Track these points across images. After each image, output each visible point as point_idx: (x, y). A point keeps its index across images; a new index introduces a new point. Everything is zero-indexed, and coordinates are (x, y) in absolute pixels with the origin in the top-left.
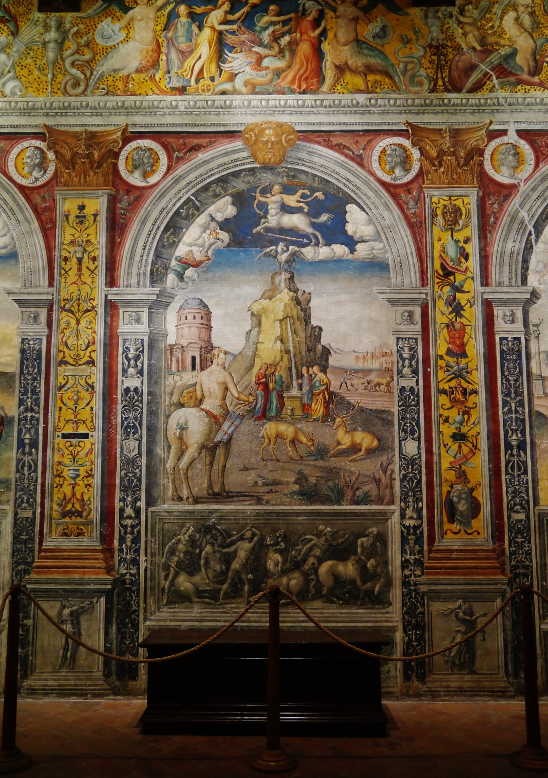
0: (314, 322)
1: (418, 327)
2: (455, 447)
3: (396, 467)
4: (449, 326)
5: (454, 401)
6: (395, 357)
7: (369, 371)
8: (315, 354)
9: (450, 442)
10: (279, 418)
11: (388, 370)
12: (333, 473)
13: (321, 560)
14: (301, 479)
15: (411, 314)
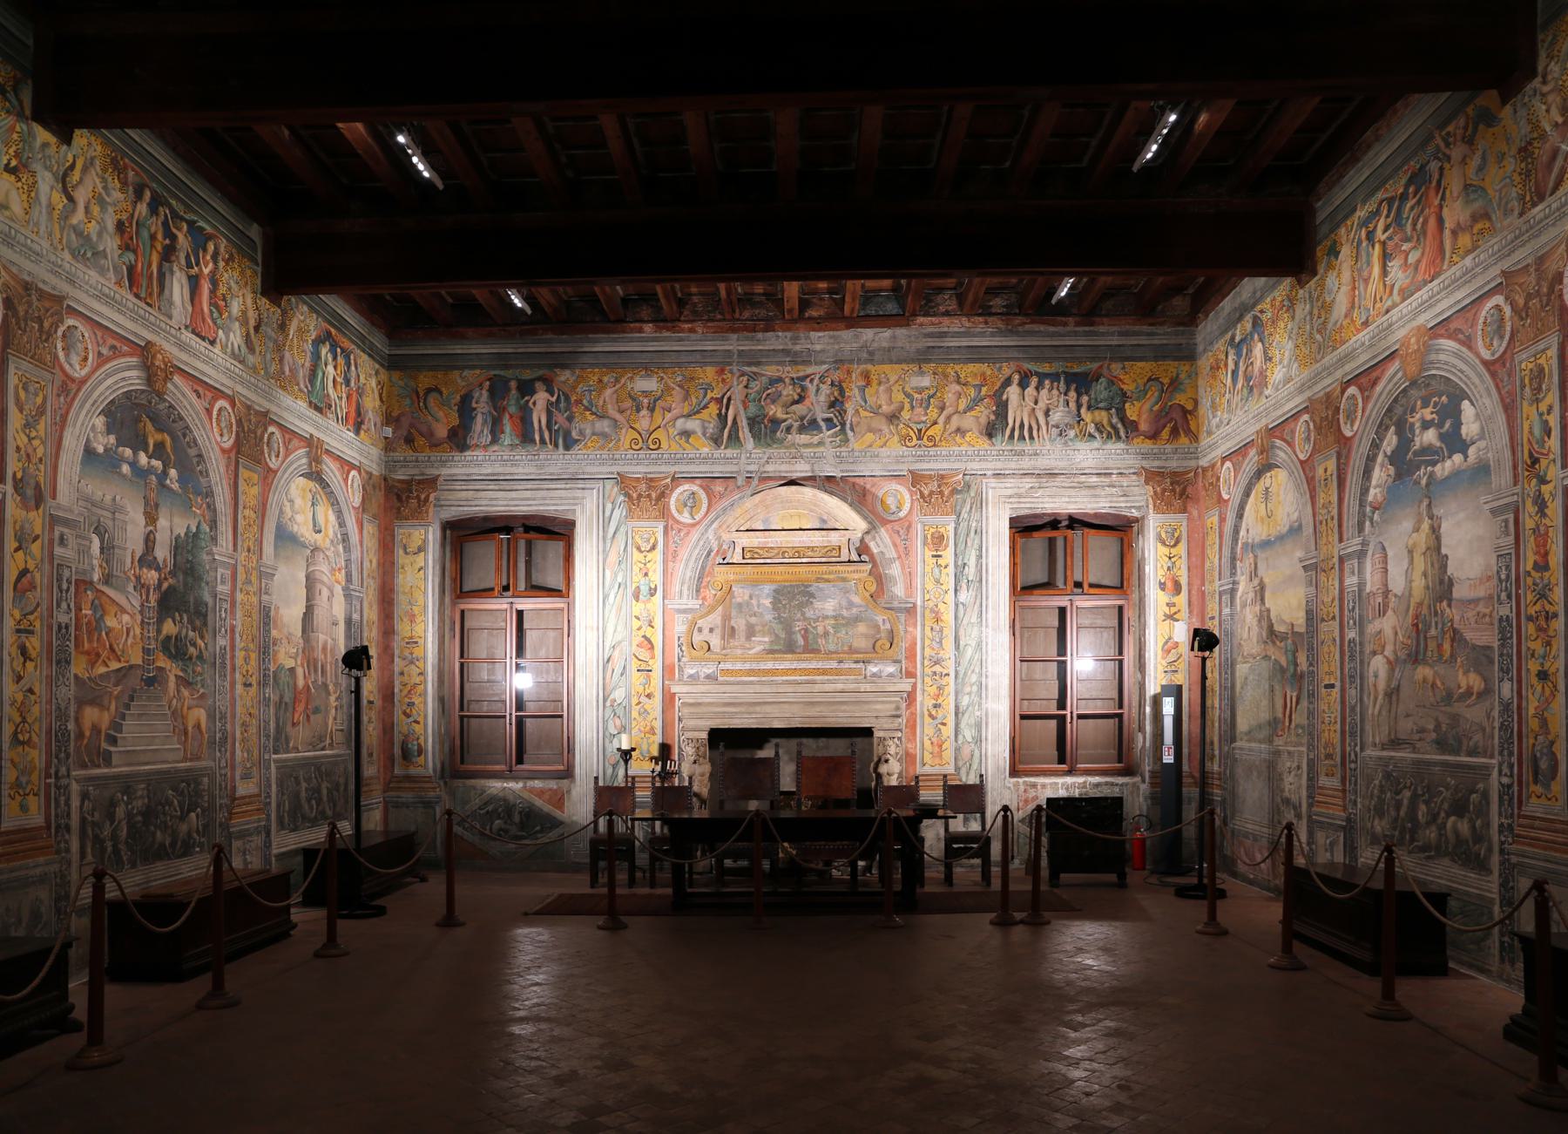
0: (1444, 551)
1: (1511, 539)
2: (1539, 688)
3: (1496, 713)
4: (1535, 531)
5: (1539, 629)
6: (1495, 581)
7: (1475, 601)
8: (1442, 588)
9: (1534, 680)
10: (1425, 662)
11: (1491, 597)
12: (1455, 719)
13: (1448, 816)
14: (1438, 727)
15: (1506, 521)
